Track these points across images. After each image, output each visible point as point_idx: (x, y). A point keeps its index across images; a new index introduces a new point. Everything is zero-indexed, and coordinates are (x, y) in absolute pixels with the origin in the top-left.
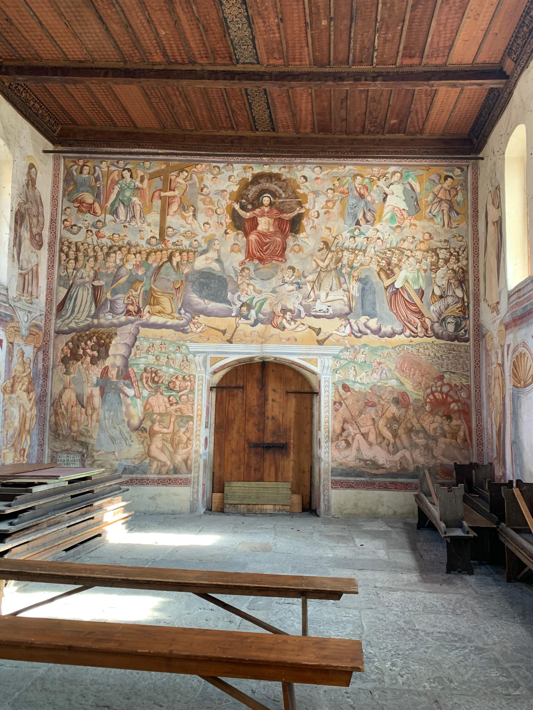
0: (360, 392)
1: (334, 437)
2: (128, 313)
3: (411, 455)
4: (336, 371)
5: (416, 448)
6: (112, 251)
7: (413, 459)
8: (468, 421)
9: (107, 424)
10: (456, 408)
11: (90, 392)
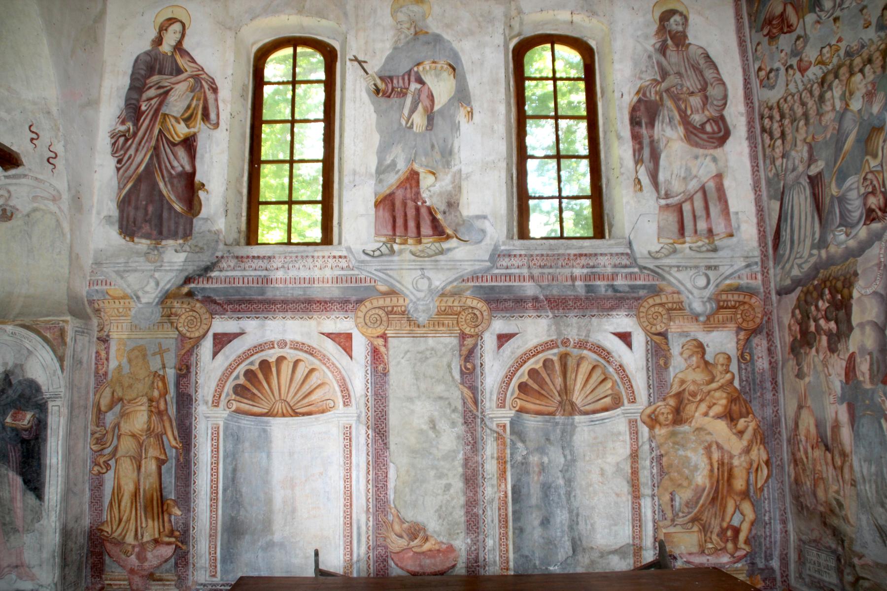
2: (870, 216)
6: (826, 86)
9: (869, 495)
11: (834, 415)
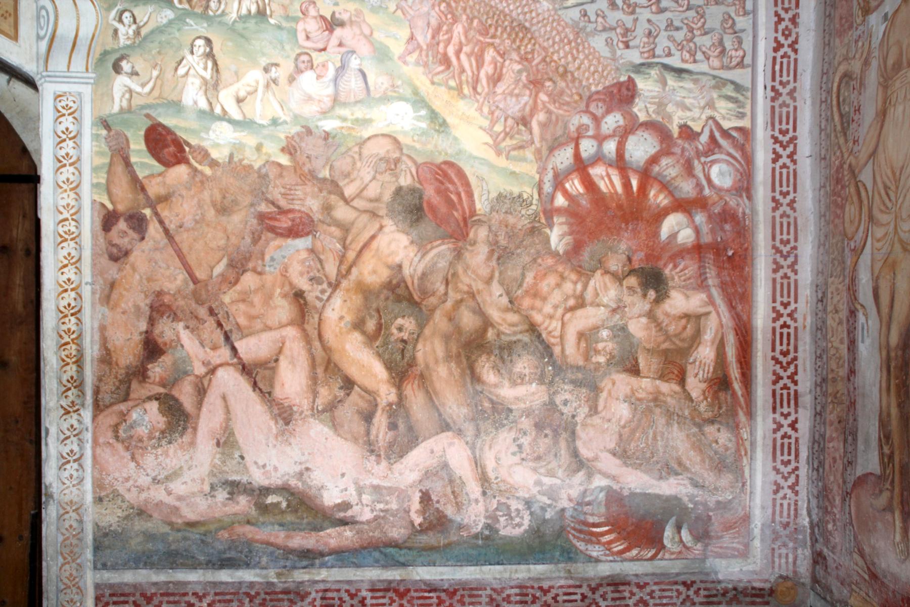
0: (235, 166)
1: (108, 387)
3: (477, 463)
4: (113, 62)
5: (499, 426)
7: (484, 479)
8: (738, 296)
10: (686, 236)
